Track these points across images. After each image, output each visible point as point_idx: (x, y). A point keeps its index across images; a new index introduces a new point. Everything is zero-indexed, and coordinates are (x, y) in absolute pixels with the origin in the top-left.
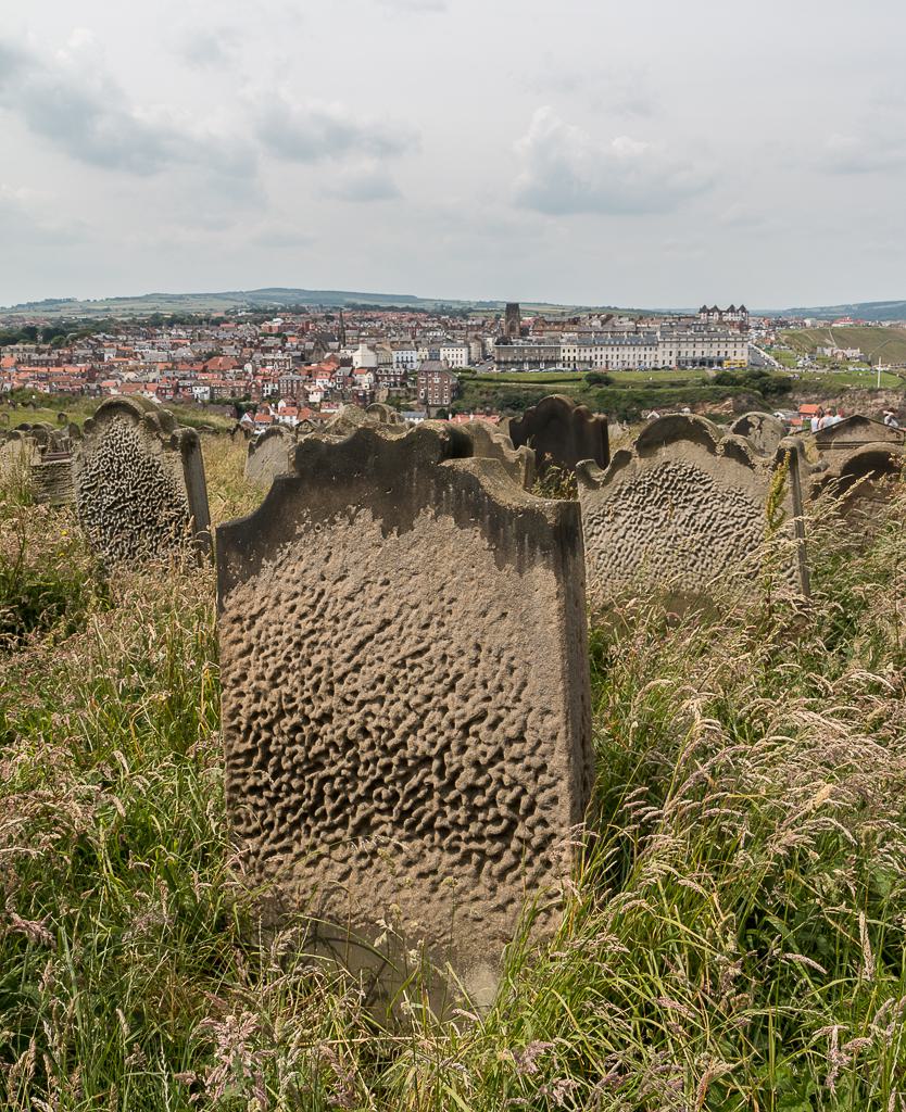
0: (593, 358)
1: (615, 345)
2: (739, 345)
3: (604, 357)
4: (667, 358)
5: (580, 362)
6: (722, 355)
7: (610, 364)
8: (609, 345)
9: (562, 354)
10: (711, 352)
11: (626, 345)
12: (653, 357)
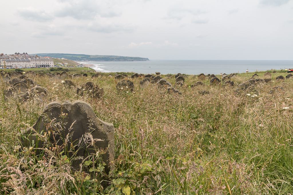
0: (12, 65)
1: (18, 61)
2: (51, 62)
3: (15, 65)
4: (33, 65)
5: (7, 66)
6: (47, 64)
7: (17, 67)
8: (16, 61)
9: (2, 64)
10: (44, 63)
11: (21, 61)
12: (29, 65)
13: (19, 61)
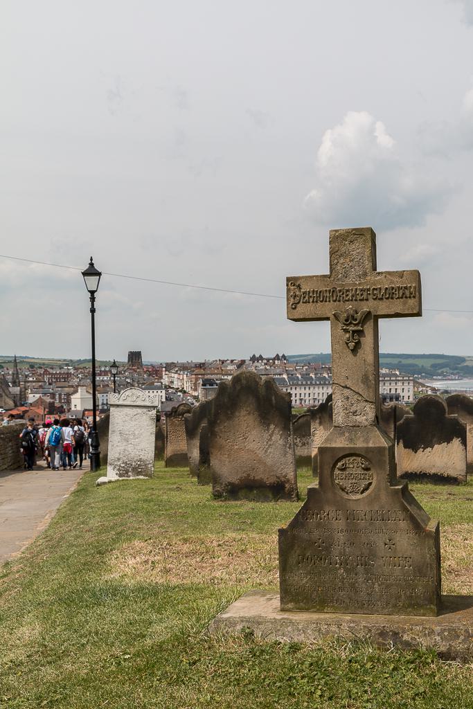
11: (316, 384)
13: (311, 384)
